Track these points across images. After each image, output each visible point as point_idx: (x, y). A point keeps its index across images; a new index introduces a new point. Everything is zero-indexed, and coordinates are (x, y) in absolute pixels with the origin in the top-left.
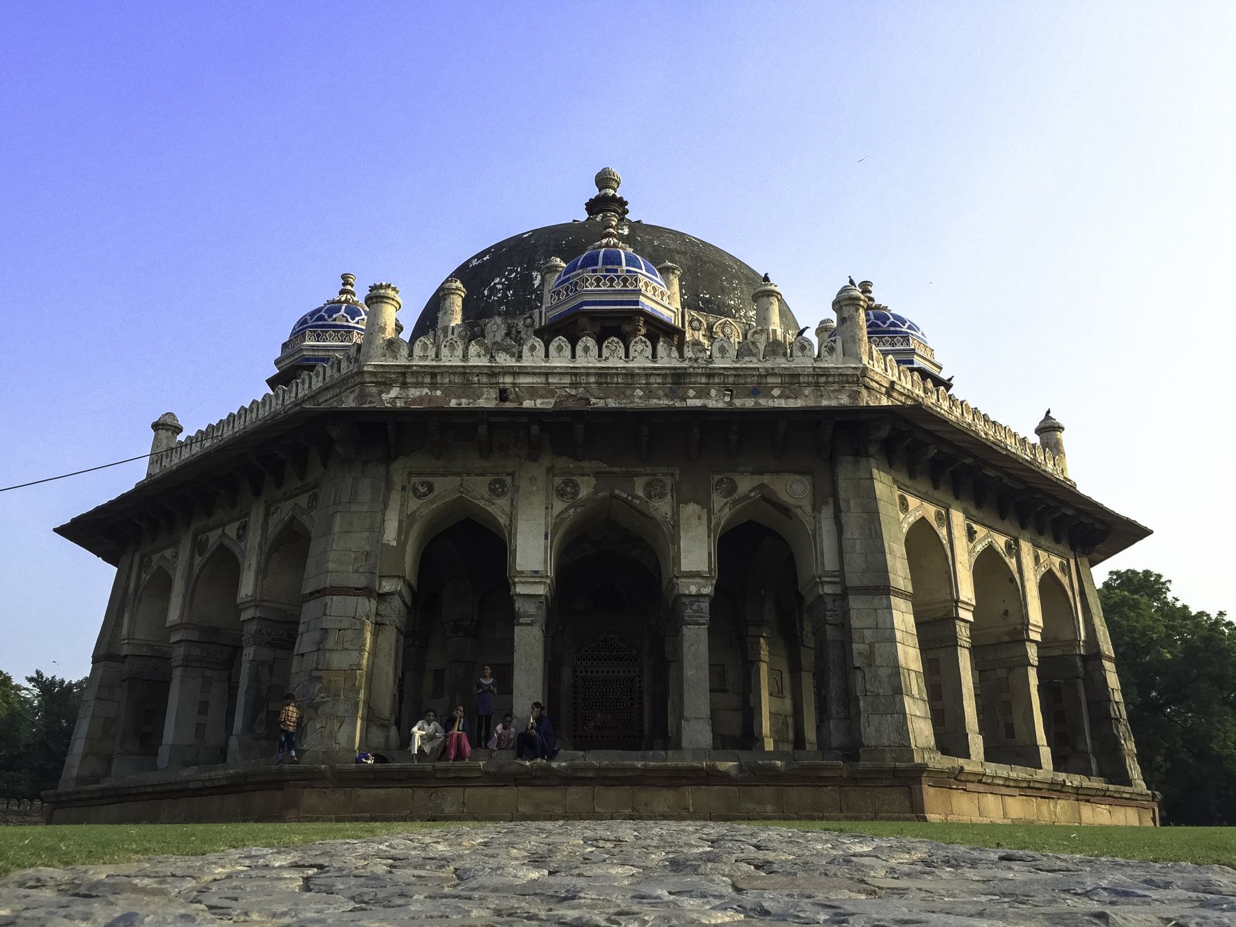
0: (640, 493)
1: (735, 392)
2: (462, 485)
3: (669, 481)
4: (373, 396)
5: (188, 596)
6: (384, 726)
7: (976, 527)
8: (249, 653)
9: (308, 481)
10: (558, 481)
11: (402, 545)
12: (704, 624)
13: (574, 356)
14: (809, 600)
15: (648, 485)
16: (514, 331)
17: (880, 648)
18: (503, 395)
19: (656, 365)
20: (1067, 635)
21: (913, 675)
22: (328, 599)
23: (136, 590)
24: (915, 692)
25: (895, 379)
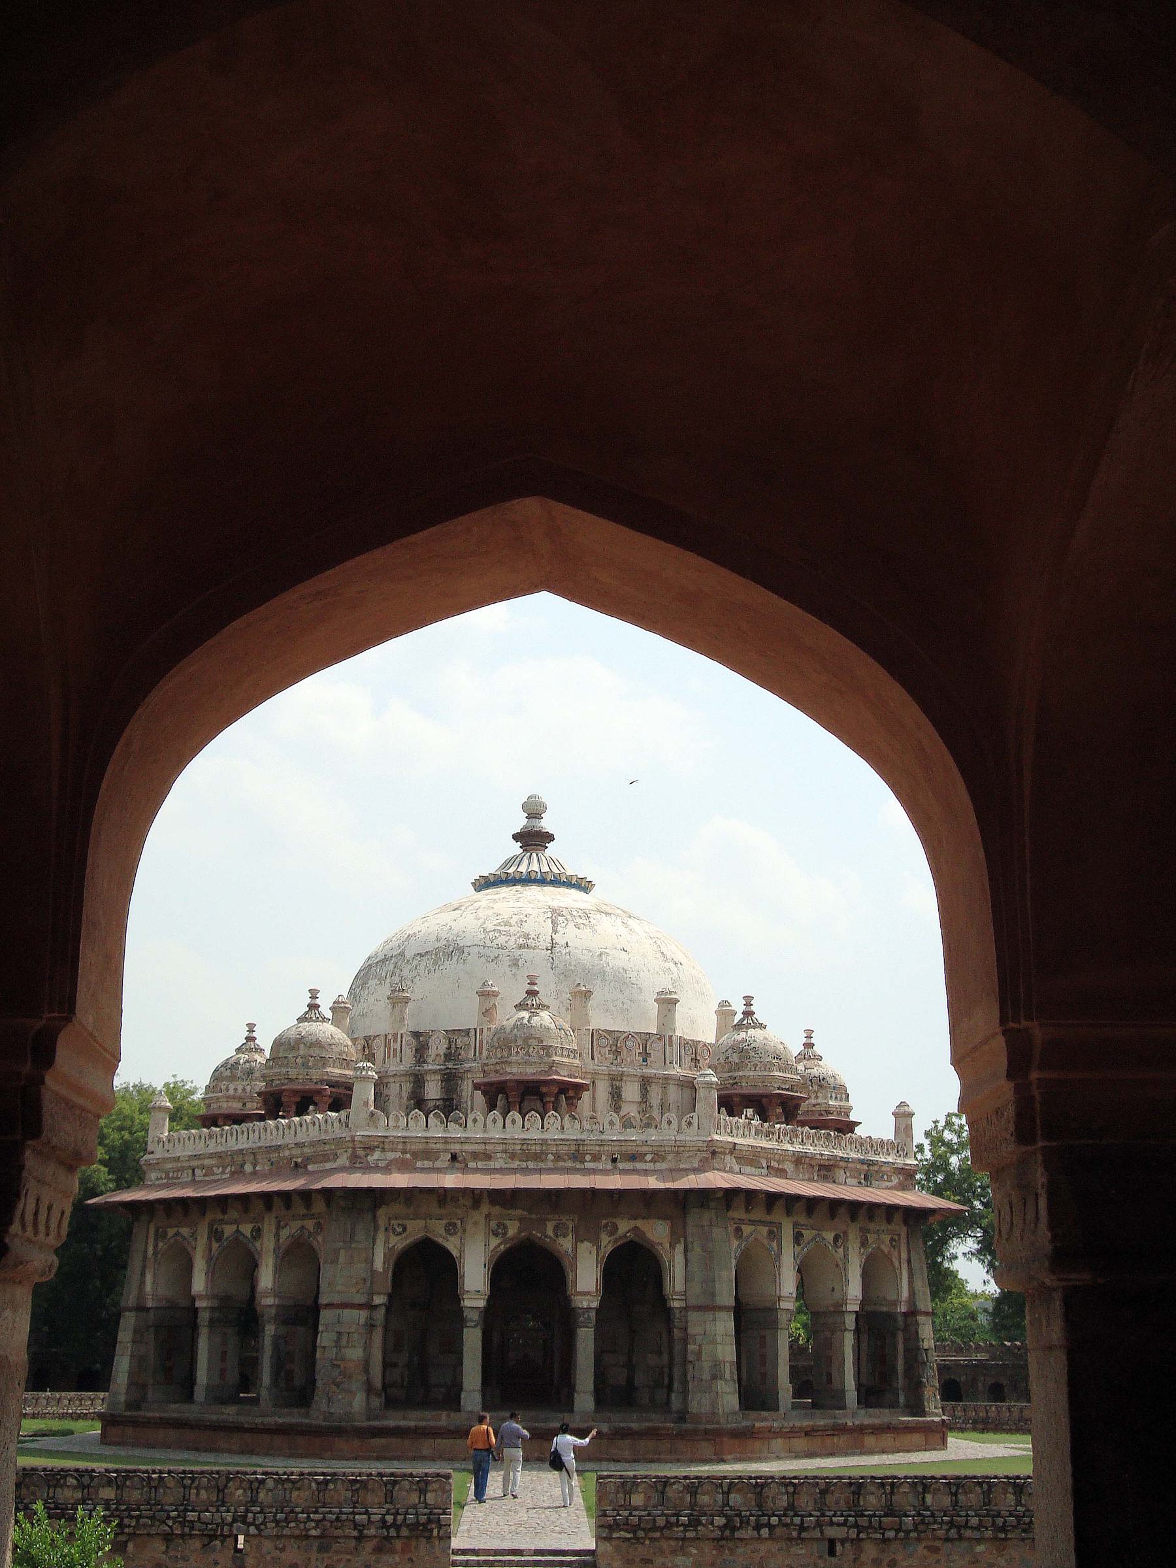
0: (552, 1235)
1: (619, 1158)
2: (426, 1226)
3: (571, 1225)
4: (360, 1158)
5: (210, 1274)
6: (379, 1395)
7: (803, 1231)
8: (270, 1330)
9: (313, 1211)
10: (493, 1224)
11: (386, 1270)
12: (592, 1328)
13: (504, 1127)
14: (668, 1306)
15: (556, 1228)
16: (453, 1046)
17: (706, 1349)
18: (454, 1157)
19: (563, 1137)
20: (892, 1297)
21: (727, 1365)
22: (340, 1311)
23: (155, 1253)
24: (728, 1375)
25: (739, 1141)
